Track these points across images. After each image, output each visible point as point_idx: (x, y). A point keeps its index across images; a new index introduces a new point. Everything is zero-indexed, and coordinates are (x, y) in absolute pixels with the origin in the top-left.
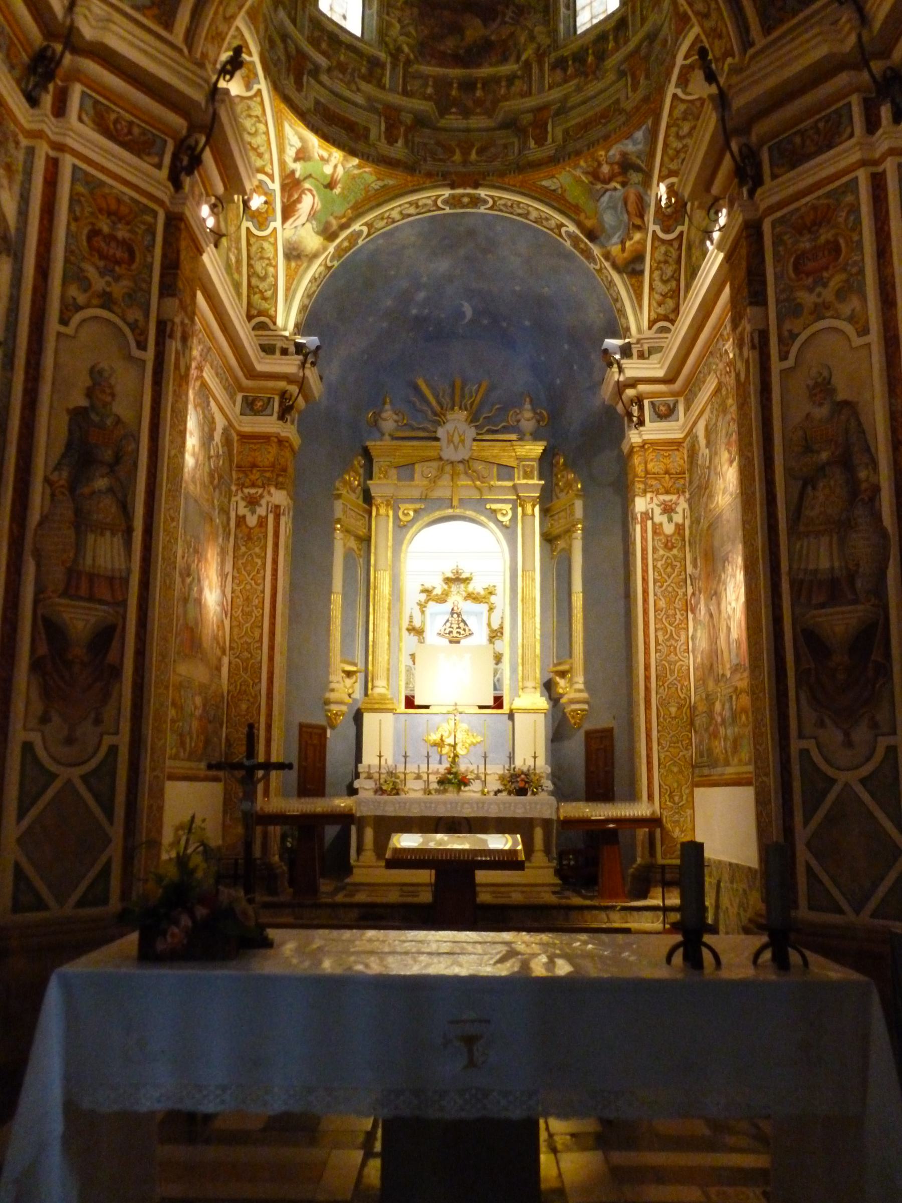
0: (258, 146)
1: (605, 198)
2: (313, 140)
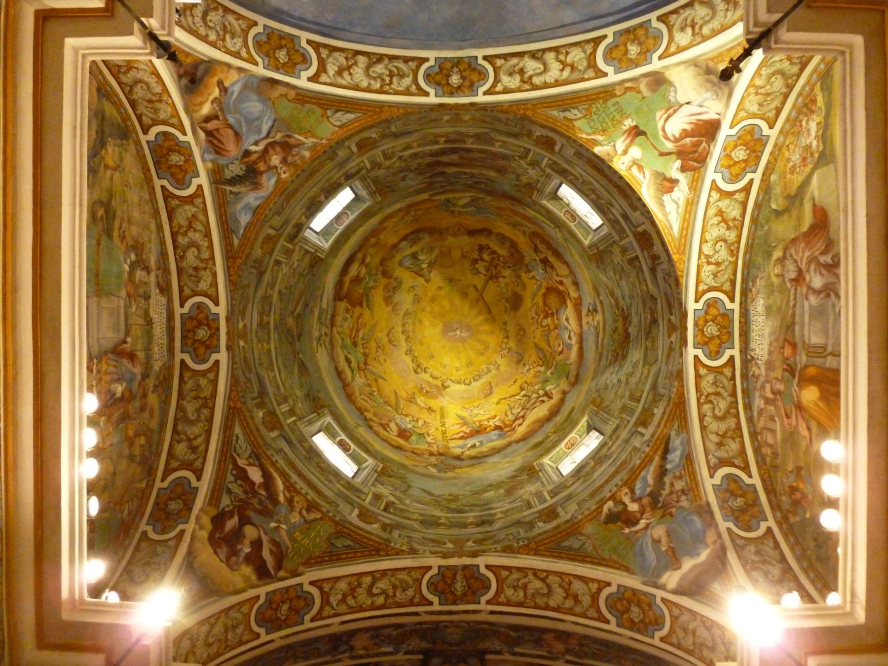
0: (718, 224)
1: (265, 129)
2: (647, 193)
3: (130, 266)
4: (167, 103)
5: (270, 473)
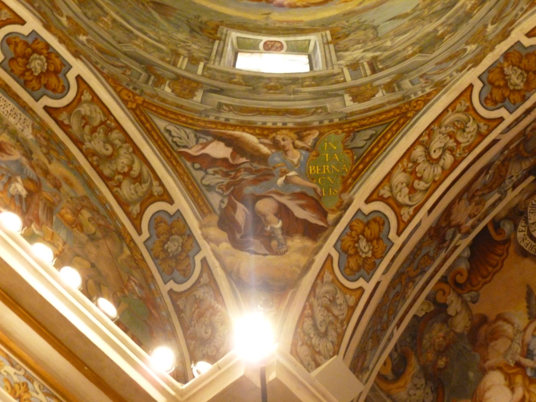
5: (231, 135)
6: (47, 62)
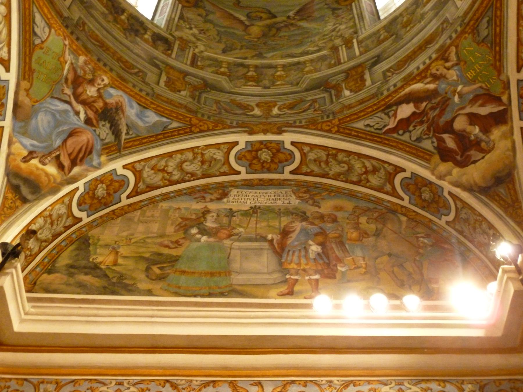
3: (203, 235)
4: (52, 210)
5: (405, 95)
6: (269, 150)
